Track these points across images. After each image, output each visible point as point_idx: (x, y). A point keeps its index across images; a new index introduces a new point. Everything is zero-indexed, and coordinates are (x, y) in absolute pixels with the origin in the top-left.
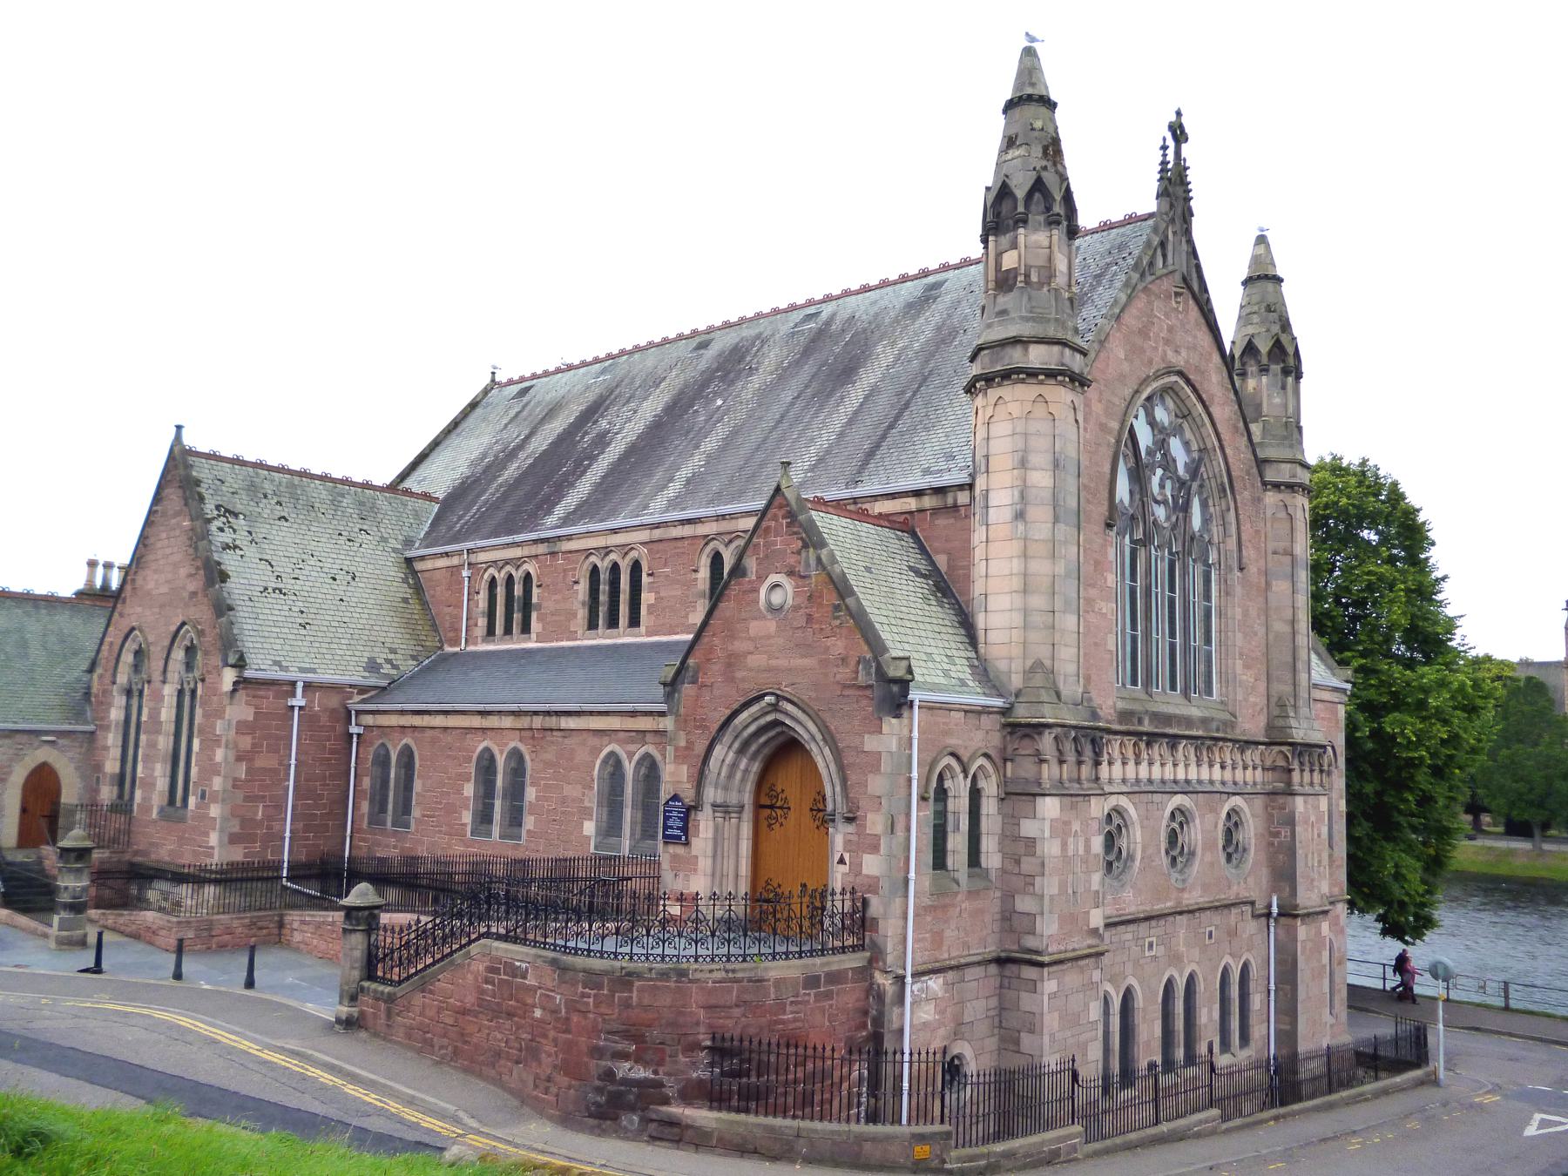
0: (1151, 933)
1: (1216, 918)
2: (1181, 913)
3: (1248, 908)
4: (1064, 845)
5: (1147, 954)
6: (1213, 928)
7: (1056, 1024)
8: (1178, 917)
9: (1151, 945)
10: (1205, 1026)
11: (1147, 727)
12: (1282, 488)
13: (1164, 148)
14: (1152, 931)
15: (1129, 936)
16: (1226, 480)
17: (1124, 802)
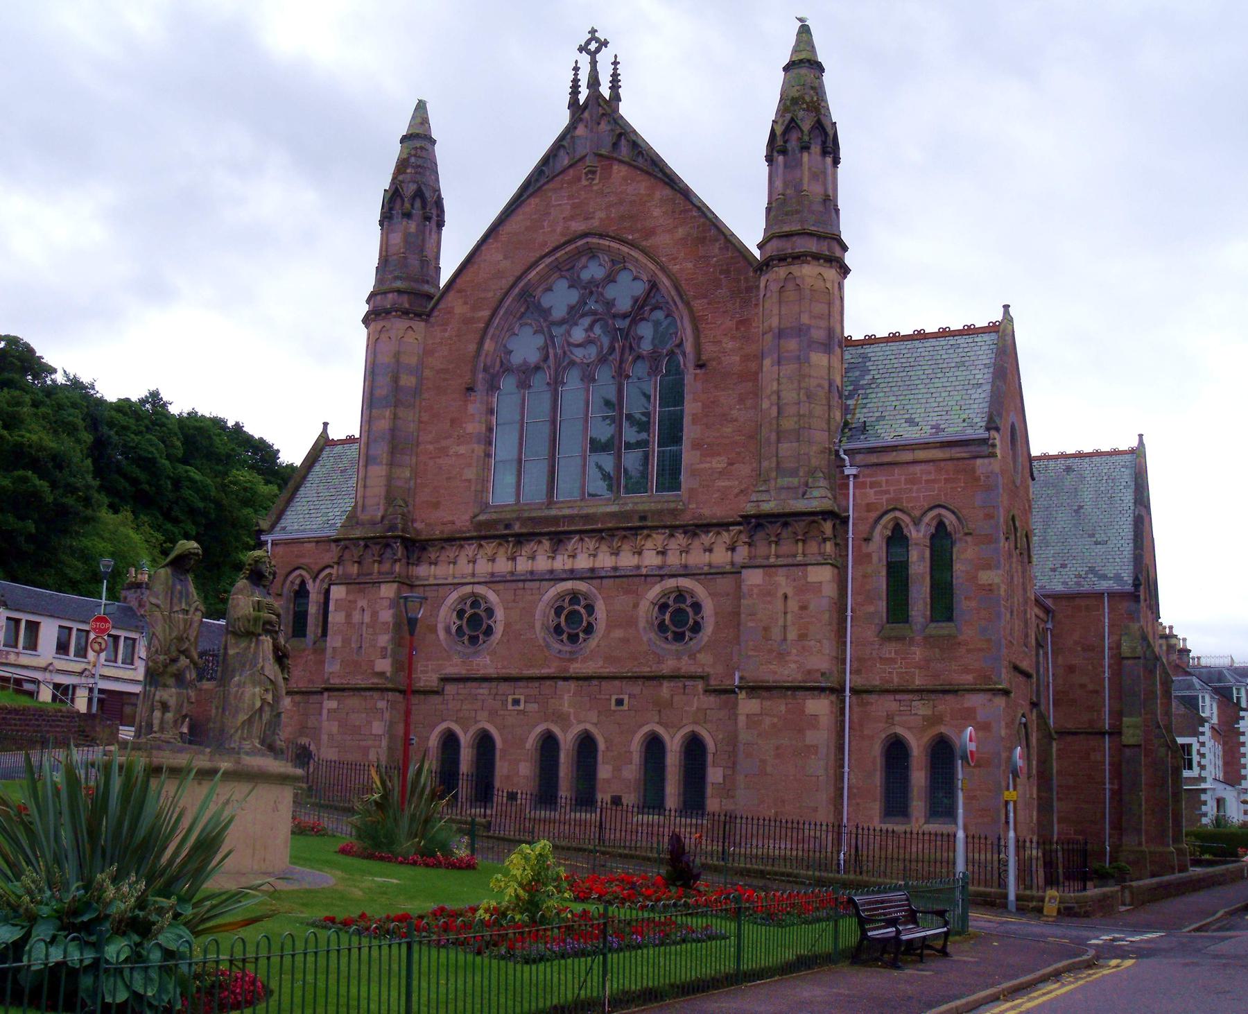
0: (520, 692)
1: (636, 689)
2: (565, 679)
3: (700, 685)
4: (349, 616)
5: (510, 707)
6: (626, 698)
7: (335, 730)
8: (561, 683)
9: (516, 702)
10: (608, 781)
11: (517, 528)
12: (822, 261)
13: (576, 69)
14: (517, 691)
15: (485, 691)
16: (673, 293)
17: (481, 590)
